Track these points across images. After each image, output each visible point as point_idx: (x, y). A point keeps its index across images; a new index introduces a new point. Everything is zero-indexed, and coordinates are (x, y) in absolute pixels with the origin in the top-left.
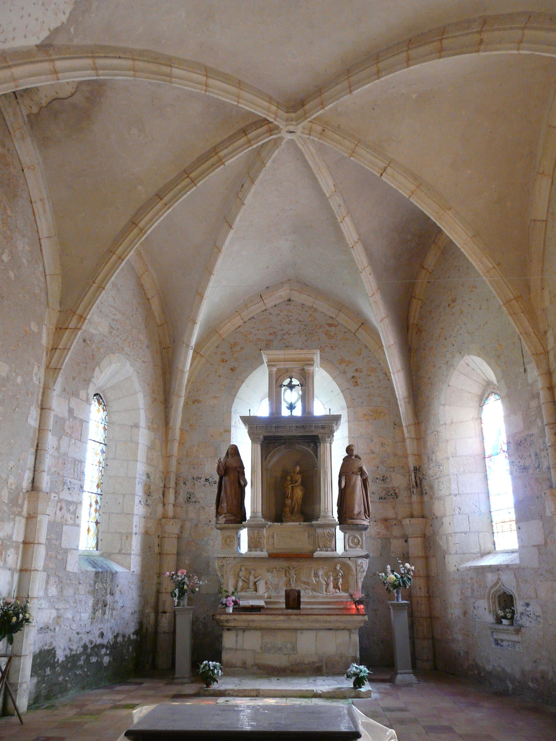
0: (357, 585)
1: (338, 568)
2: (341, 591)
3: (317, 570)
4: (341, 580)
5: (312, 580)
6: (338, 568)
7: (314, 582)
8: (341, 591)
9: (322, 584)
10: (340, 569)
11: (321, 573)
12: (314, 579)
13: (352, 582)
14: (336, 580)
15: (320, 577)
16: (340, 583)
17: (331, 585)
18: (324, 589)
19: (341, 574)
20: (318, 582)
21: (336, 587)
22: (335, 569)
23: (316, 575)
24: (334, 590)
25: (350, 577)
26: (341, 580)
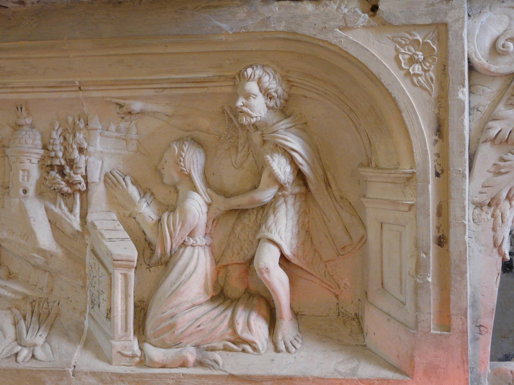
0: (449, 273)
1: (258, 108)
2: (287, 326)
3: (69, 132)
4: (283, 228)
5: (30, 234)
6: (258, 108)
7: (45, 238)
8: (287, 326)
9: (105, 263)
10: (284, 109)
11: (101, 156)
12: (37, 214)
13: (396, 243)
14: (239, 217)
15: (99, 194)
16: (269, 258)
17: (196, 268)
18: (122, 307)
19: (281, 168)
20: (78, 244)
21: (237, 288)
22: (232, 115)
23: (61, 179)
24: (214, 320)
25: (378, 189)
26: (283, 228)
